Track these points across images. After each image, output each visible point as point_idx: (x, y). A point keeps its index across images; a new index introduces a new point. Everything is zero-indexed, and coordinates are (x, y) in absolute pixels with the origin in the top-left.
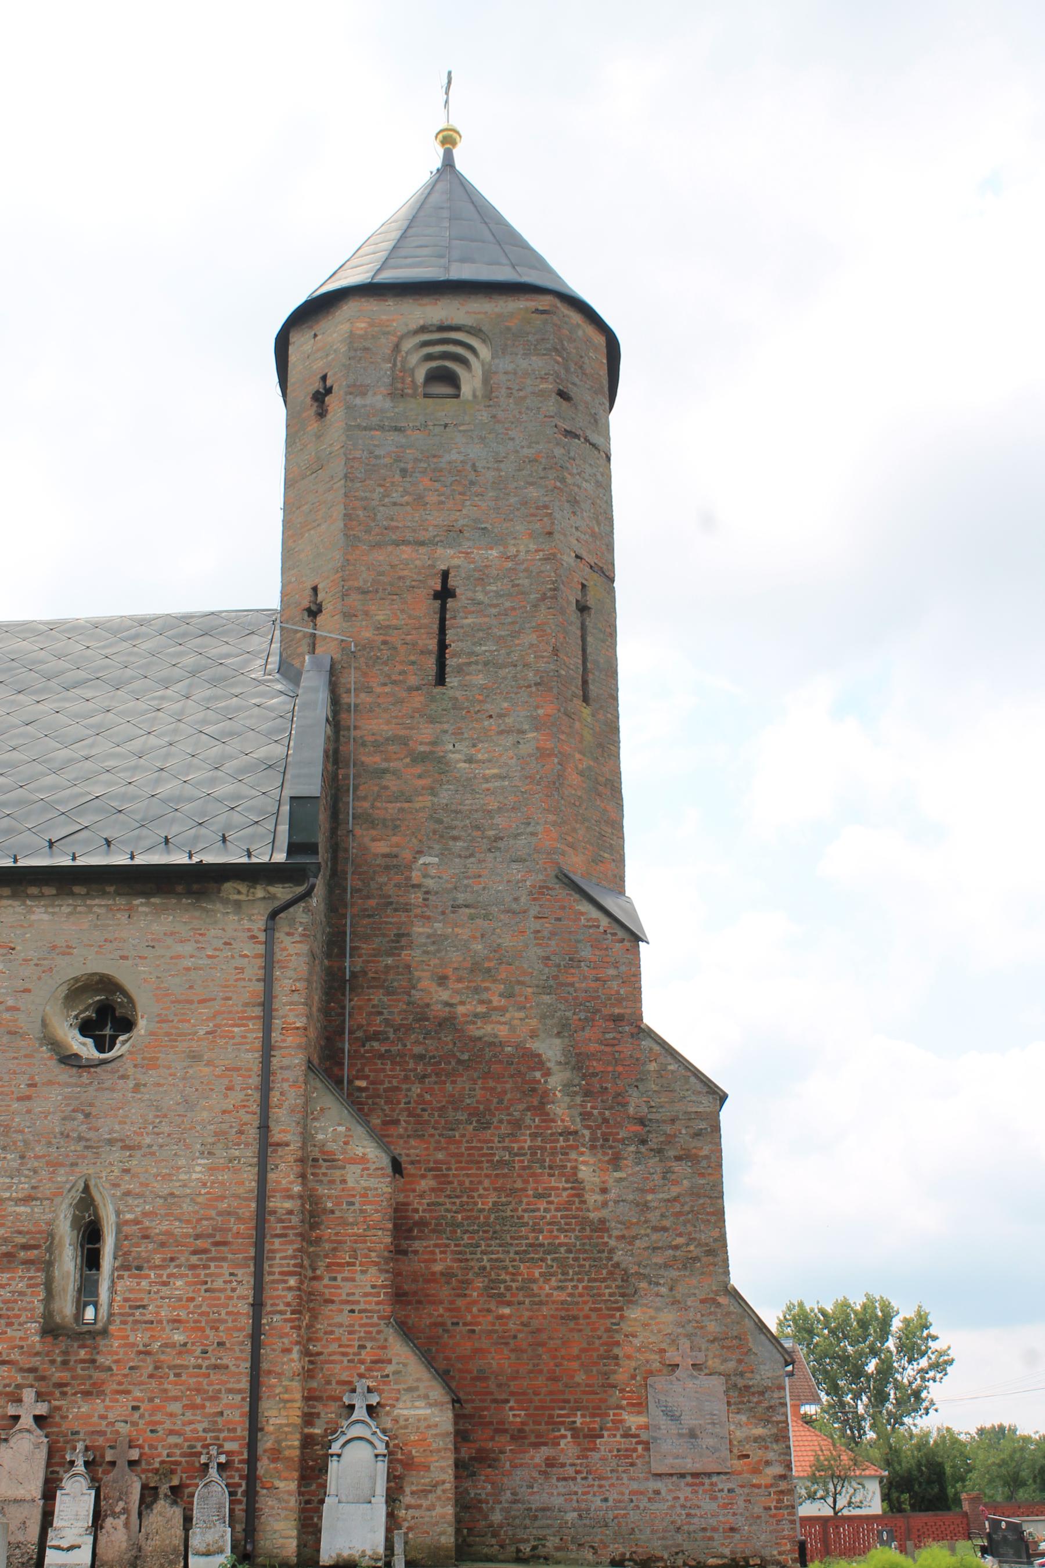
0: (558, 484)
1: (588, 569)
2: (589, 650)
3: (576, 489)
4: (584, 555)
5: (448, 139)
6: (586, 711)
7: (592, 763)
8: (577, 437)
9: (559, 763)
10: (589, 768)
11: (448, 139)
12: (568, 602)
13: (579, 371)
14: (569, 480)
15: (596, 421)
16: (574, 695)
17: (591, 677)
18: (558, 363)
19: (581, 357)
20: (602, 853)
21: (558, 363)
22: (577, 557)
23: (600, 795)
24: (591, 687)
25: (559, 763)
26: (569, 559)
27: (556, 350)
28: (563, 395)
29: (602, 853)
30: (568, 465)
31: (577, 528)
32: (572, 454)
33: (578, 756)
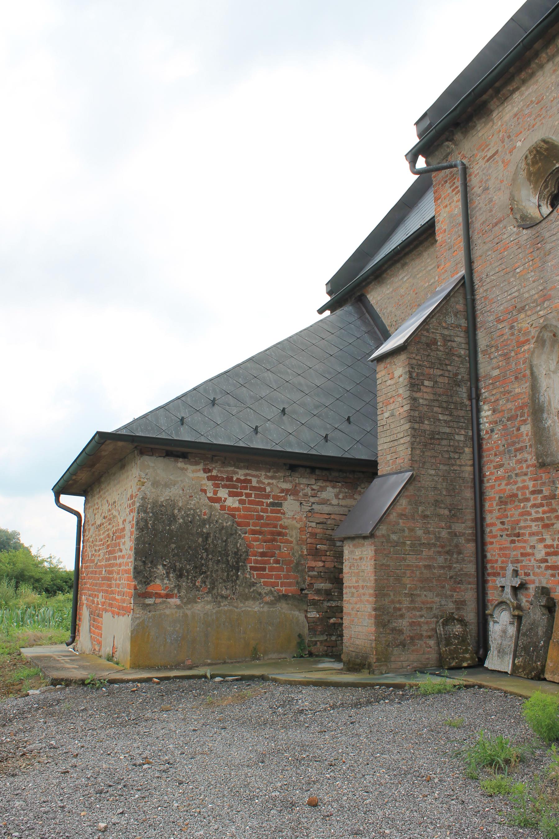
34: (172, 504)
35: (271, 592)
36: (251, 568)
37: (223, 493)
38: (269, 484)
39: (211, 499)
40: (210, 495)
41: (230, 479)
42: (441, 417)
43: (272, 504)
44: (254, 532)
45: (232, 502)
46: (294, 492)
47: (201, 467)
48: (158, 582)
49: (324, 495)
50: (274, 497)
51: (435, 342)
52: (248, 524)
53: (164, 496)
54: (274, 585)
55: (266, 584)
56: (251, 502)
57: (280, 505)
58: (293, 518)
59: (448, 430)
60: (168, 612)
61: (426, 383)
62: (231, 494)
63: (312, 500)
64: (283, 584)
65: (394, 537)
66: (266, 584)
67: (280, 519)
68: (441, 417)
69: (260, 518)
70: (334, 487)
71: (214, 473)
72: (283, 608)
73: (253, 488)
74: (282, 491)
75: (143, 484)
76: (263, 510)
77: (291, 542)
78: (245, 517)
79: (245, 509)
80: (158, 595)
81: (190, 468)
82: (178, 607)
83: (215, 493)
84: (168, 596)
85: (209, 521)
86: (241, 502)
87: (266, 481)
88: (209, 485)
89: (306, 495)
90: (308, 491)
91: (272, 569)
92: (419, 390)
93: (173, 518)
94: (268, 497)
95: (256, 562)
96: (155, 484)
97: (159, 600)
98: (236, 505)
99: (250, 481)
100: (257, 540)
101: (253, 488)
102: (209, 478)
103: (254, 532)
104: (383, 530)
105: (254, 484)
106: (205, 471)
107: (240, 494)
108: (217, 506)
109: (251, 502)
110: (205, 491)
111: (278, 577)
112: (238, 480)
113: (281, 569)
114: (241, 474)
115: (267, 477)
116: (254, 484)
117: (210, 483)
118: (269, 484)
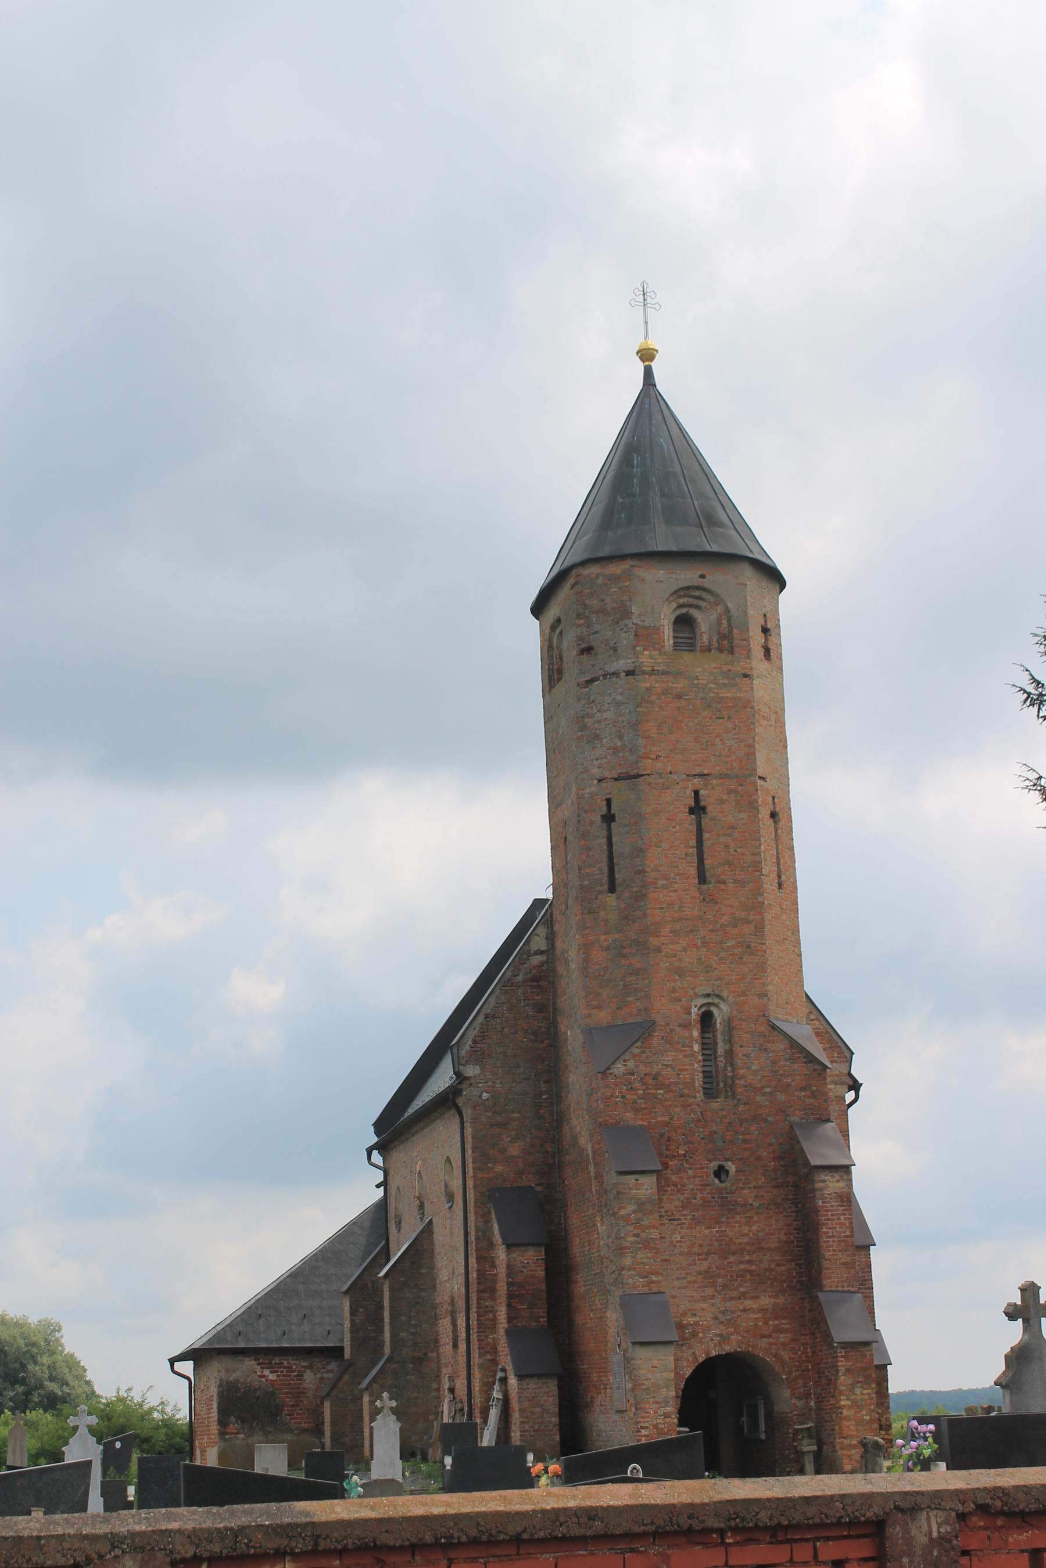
0: (580, 734)
1: (614, 782)
2: (614, 848)
3: (597, 726)
4: (607, 774)
5: (647, 355)
6: (611, 900)
7: (617, 936)
8: (597, 679)
9: (584, 953)
10: (615, 941)
11: (647, 355)
12: (591, 823)
13: (601, 616)
14: (589, 722)
15: (615, 650)
16: (600, 892)
17: (616, 868)
18: (580, 626)
19: (603, 601)
20: (627, 999)
21: (580, 626)
22: (600, 781)
23: (624, 956)
24: (617, 876)
25: (584, 953)
26: (592, 788)
27: (579, 616)
28: (589, 650)
29: (627, 999)
30: (589, 711)
31: (597, 759)
32: (592, 698)
33: (602, 938)
34: (237, 1381)
35: (298, 1428)
36: (286, 1414)
37: (266, 1372)
38: (294, 1364)
39: (260, 1376)
40: (258, 1374)
41: (270, 1363)
42: (369, 1328)
43: (296, 1376)
44: (286, 1393)
45: (272, 1377)
46: (310, 1367)
47: (252, 1358)
48: (232, 1426)
49: (330, 1367)
50: (298, 1371)
51: (367, 1285)
52: (282, 1389)
53: (233, 1377)
54: (300, 1423)
55: (295, 1423)
56: (284, 1376)
57: (302, 1376)
58: (310, 1383)
59: (374, 1335)
60: (237, 1442)
61: (361, 1310)
62: (271, 1372)
63: (322, 1370)
64: (305, 1423)
65: (341, 1396)
66: (295, 1423)
67: (301, 1384)
68: (369, 1328)
69: (290, 1384)
70: (336, 1361)
71: (261, 1361)
72: (305, 1436)
73: (285, 1367)
74: (303, 1367)
75: (220, 1371)
76: (291, 1380)
77: (309, 1397)
78: (281, 1385)
79: (280, 1380)
80: (232, 1433)
81: (247, 1359)
82: (243, 1439)
83: (262, 1372)
84: (238, 1433)
85: (259, 1389)
86: (278, 1376)
87: (293, 1362)
88: (258, 1368)
89: (318, 1368)
90: (320, 1365)
91: (298, 1414)
92: (356, 1315)
93: (238, 1390)
94: (294, 1371)
95: (288, 1410)
96: (227, 1371)
97: (232, 1436)
98: (275, 1378)
99: (283, 1363)
100: (289, 1398)
101: (285, 1367)
102: (258, 1364)
103: (286, 1393)
104: (335, 1392)
105: (285, 1364)
106: (256, 1360)
107: (277, 1372)
108: (264, 1380)
109: (284, 1376)
110: (256, 1372)
111: (302, 1419)
112: (276, 1363)
113: (303, 1414)
114: (277, 1360)
115: (293, 1360)
116: (285, 1364)
117: (259, 1367)
118: (294, 1364)
